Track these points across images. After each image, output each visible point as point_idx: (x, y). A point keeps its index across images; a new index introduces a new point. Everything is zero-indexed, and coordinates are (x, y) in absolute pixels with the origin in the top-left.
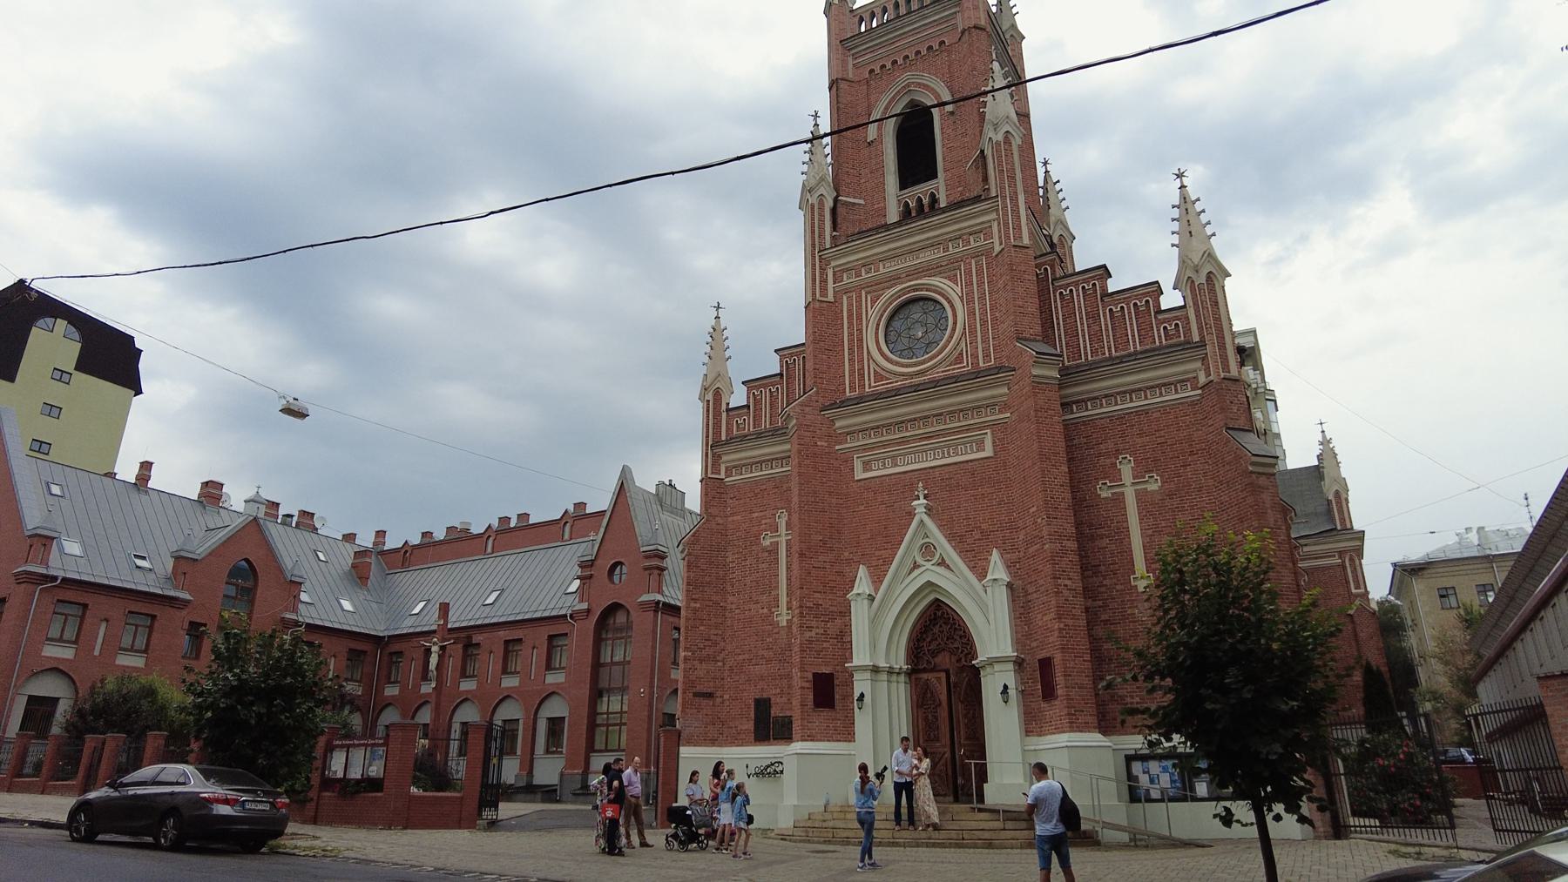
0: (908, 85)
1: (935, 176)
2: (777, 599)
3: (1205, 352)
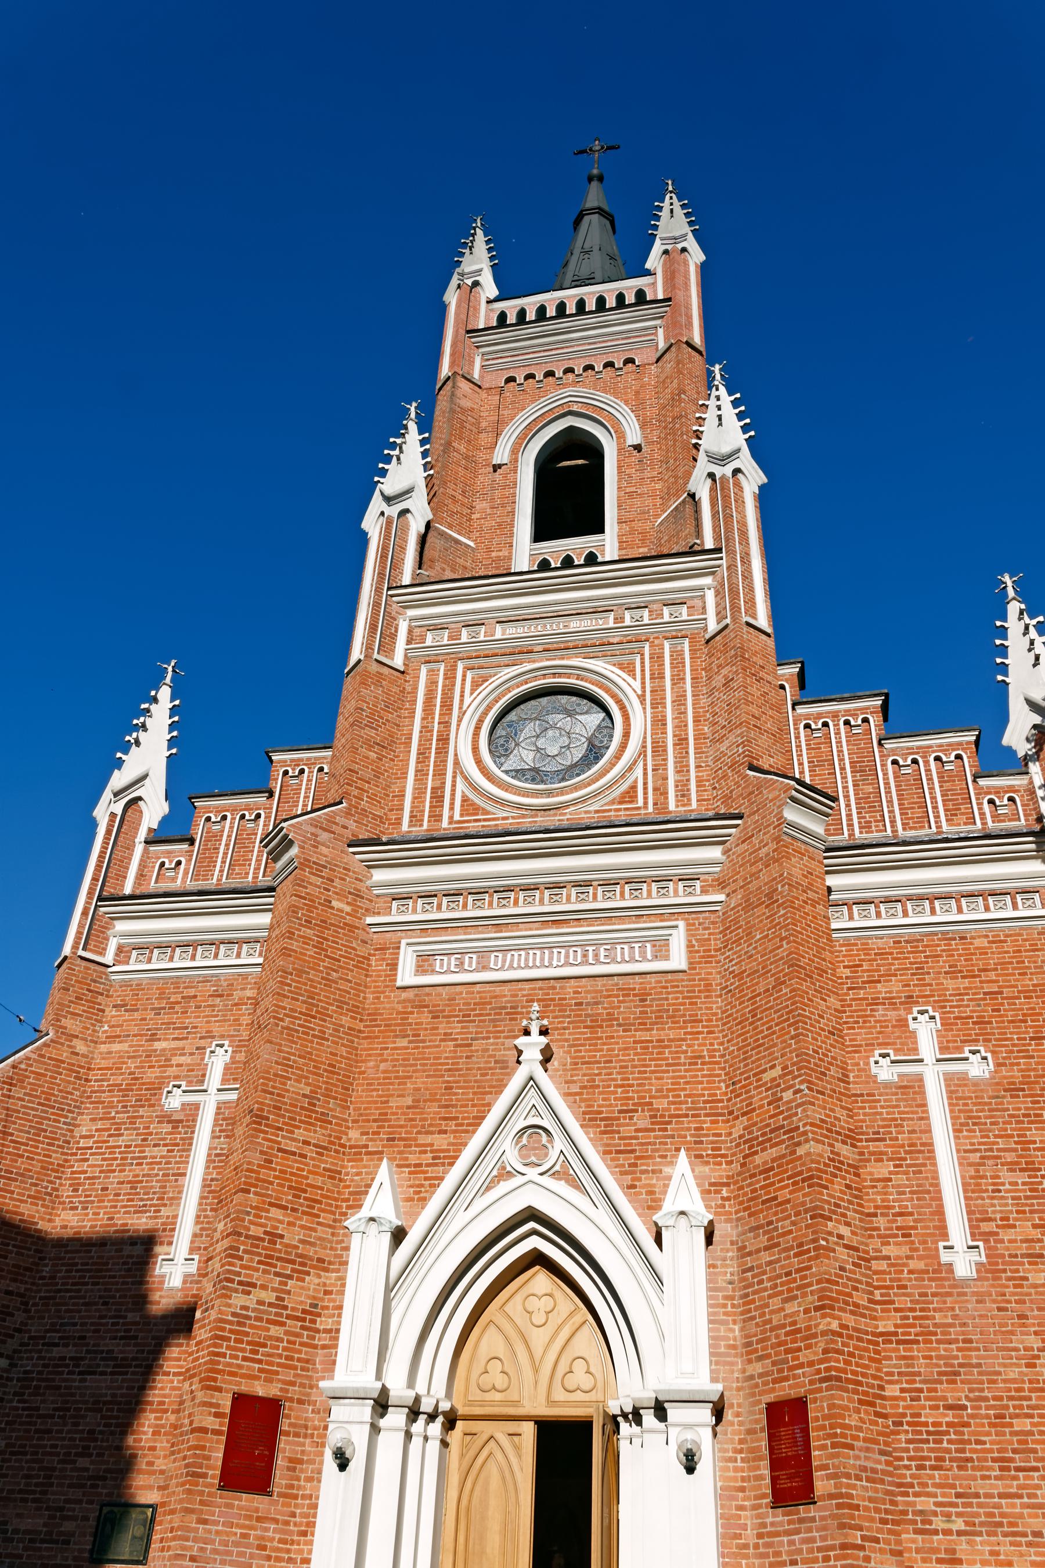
1: (601, 531)
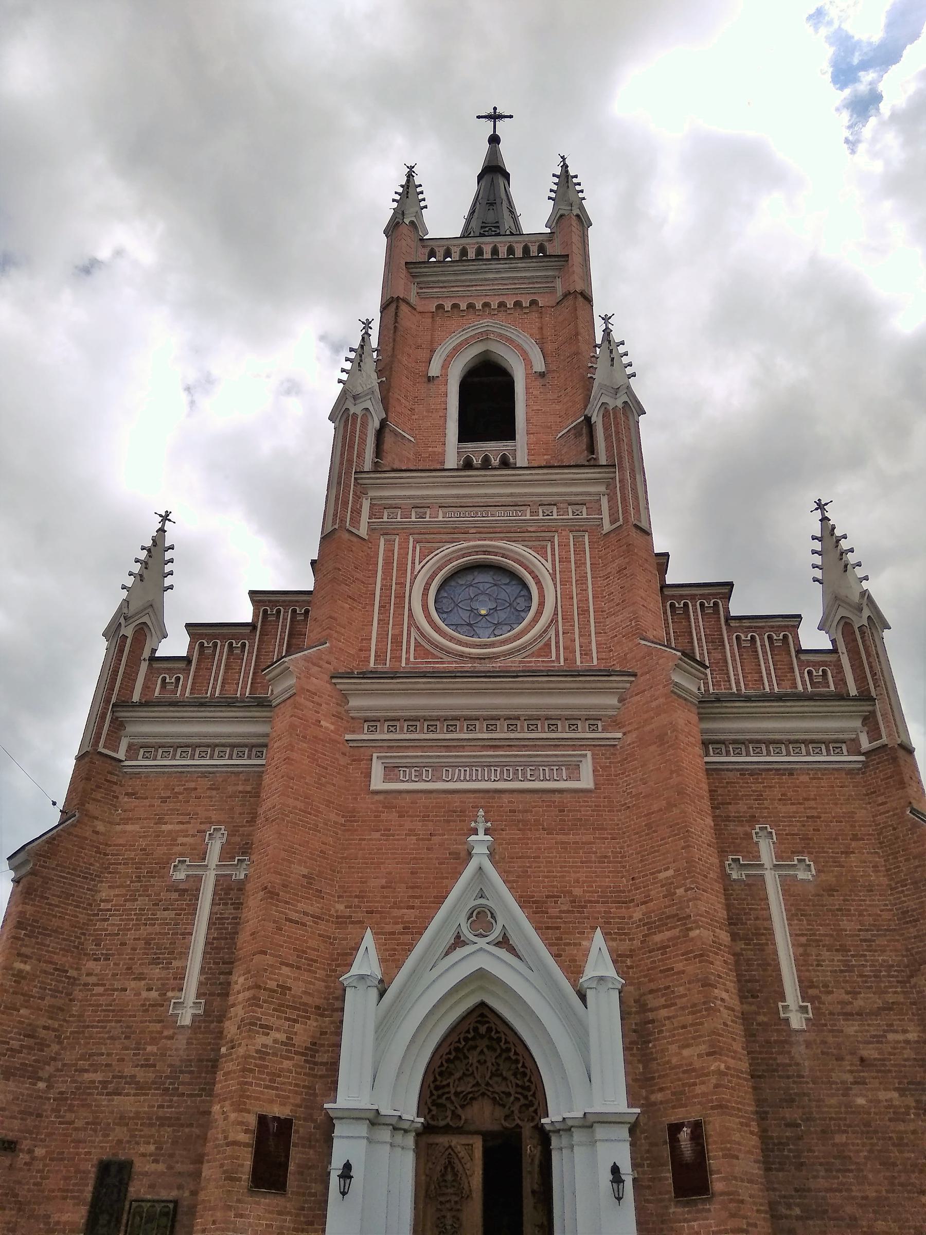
2: (180, 976)
3: (870, 708)
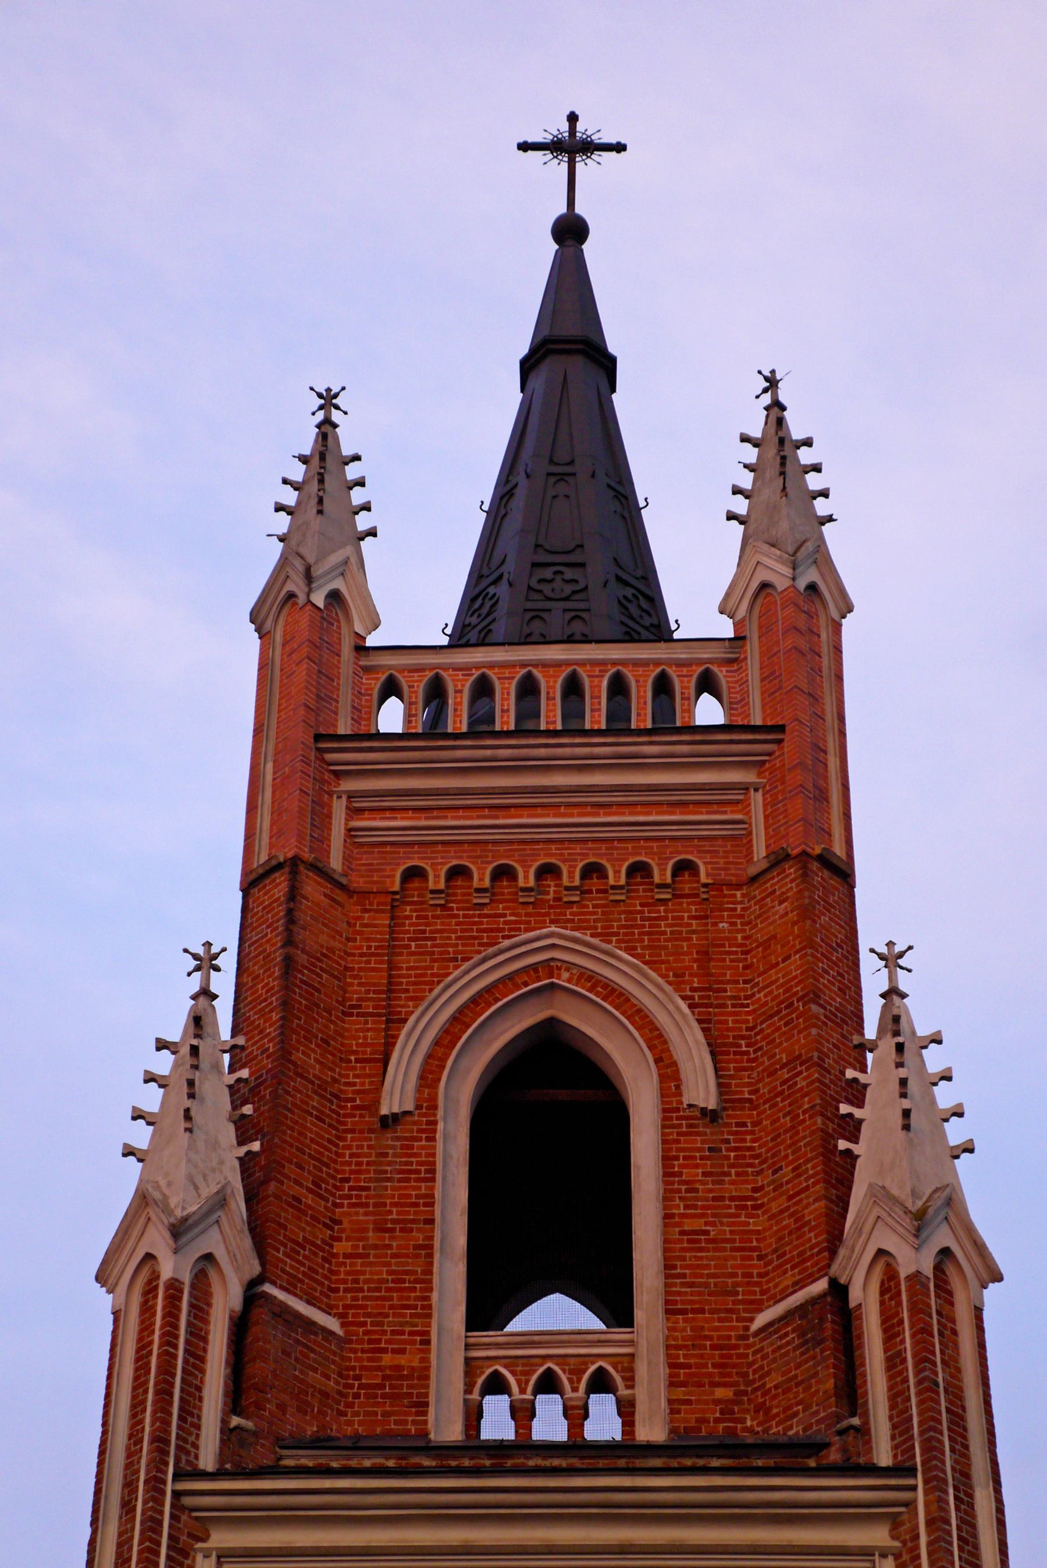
0: (549, 968)
